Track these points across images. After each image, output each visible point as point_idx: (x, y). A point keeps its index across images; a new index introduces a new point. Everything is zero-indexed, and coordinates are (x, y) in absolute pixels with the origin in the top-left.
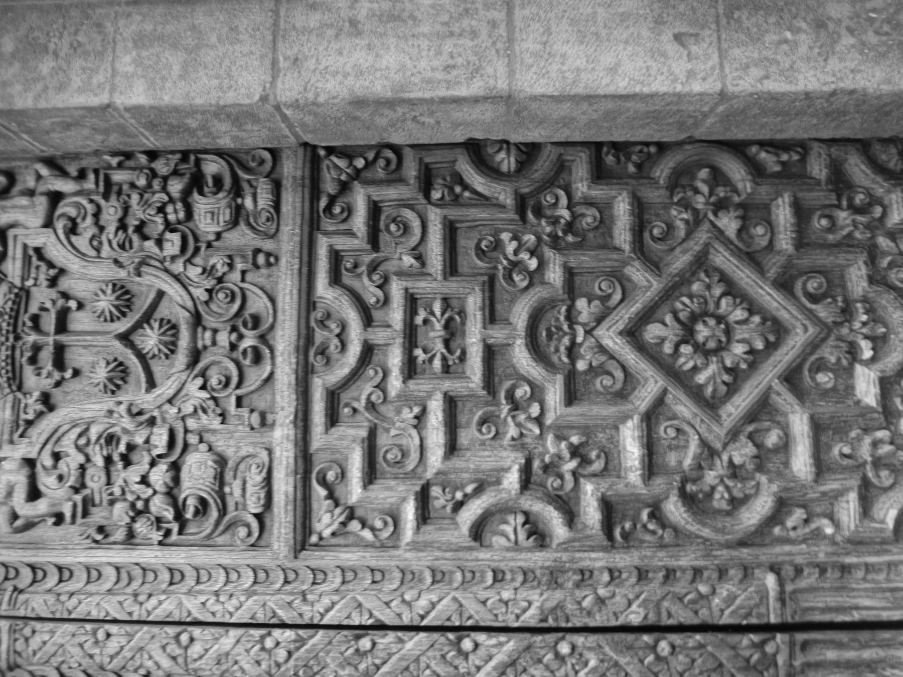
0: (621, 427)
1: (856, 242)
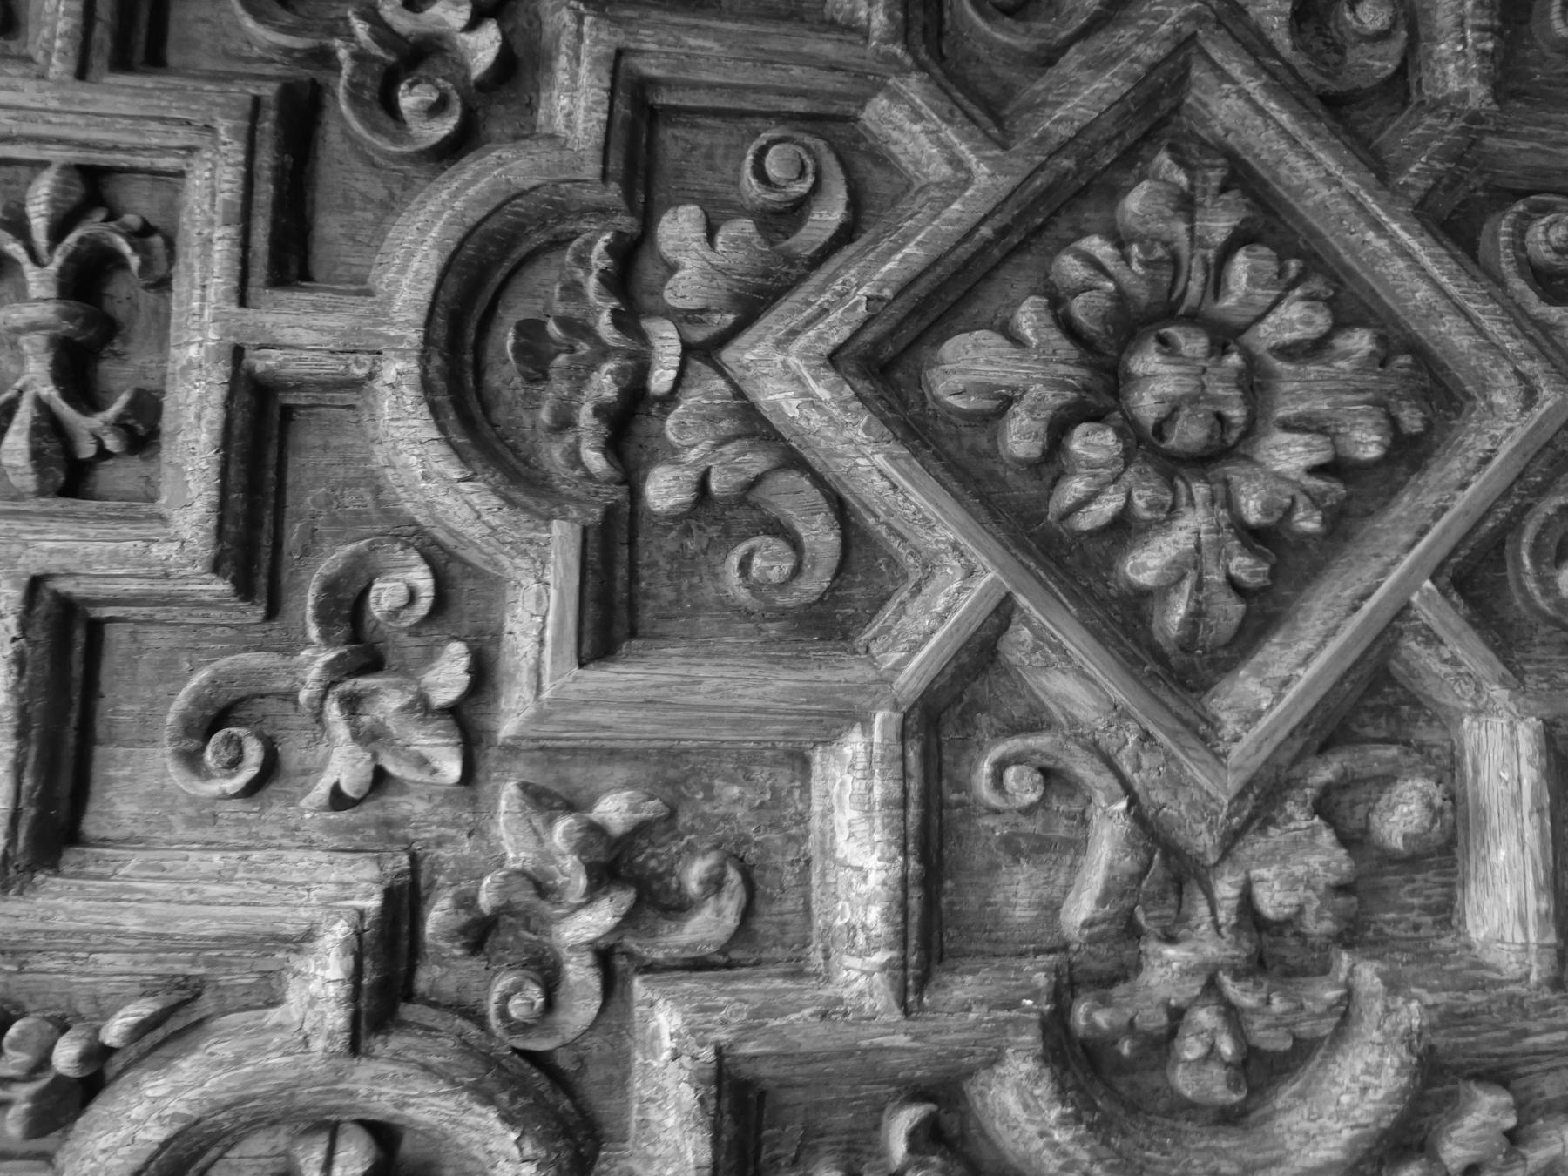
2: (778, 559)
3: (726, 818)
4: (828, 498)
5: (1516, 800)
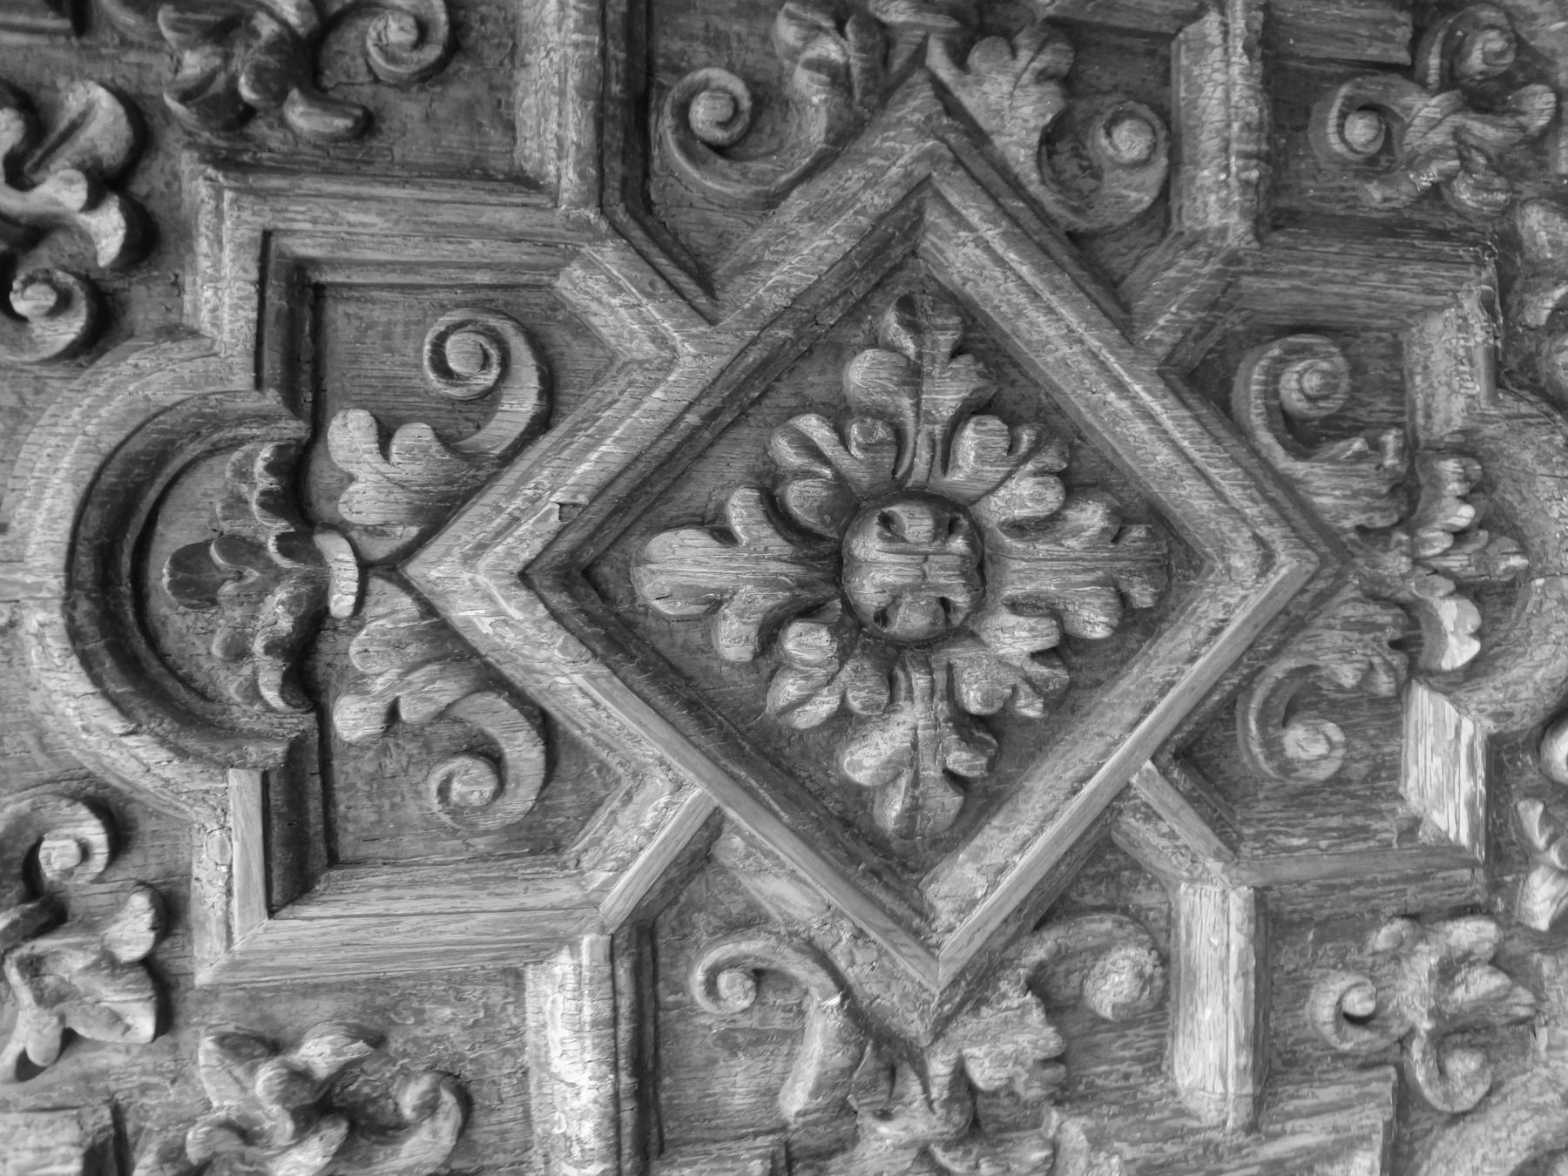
1: (1452, 223)
2: (478, 783)
3: (438, 1040)
4: (528, 716)
5: (1223, 965)
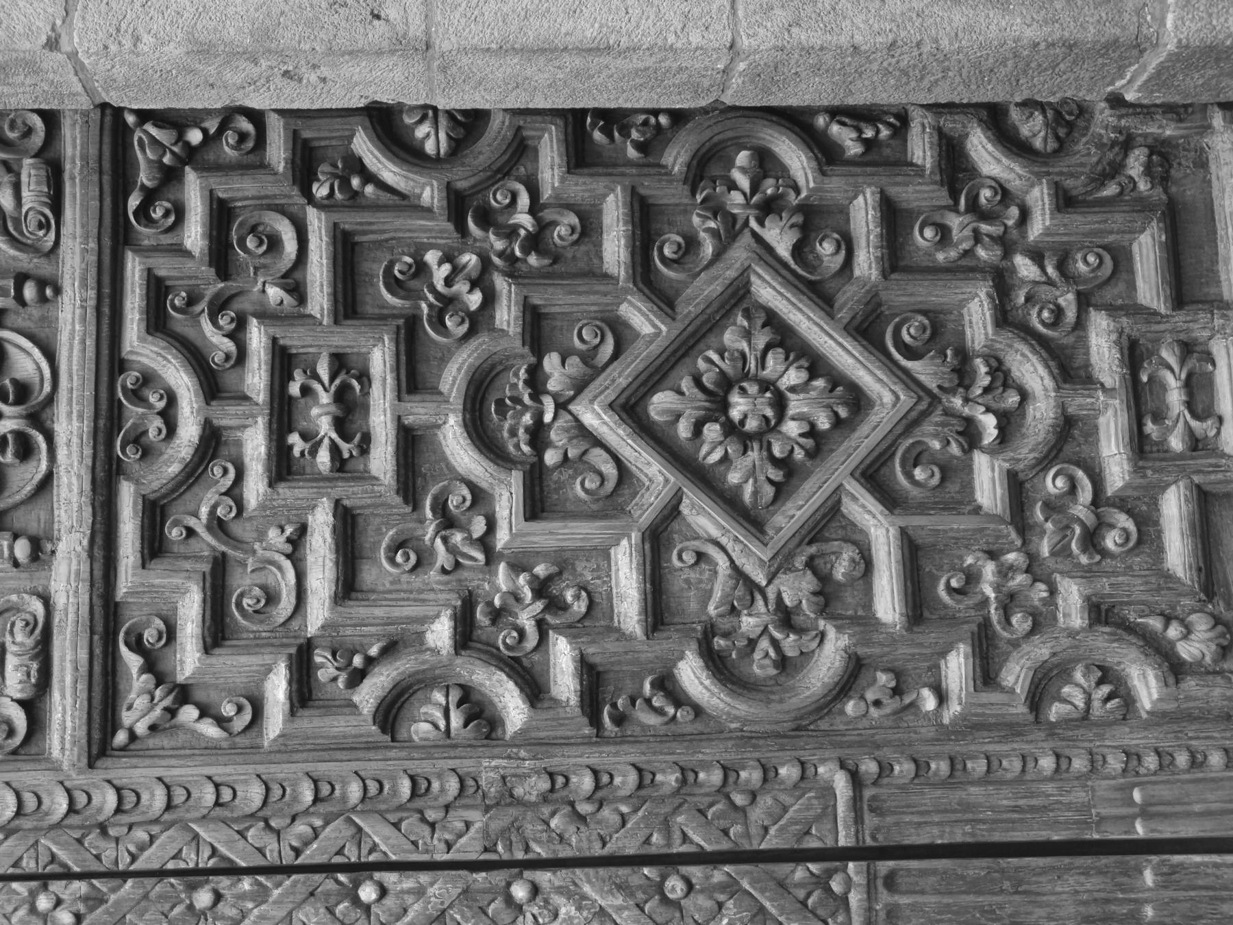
0: (612, 551)
